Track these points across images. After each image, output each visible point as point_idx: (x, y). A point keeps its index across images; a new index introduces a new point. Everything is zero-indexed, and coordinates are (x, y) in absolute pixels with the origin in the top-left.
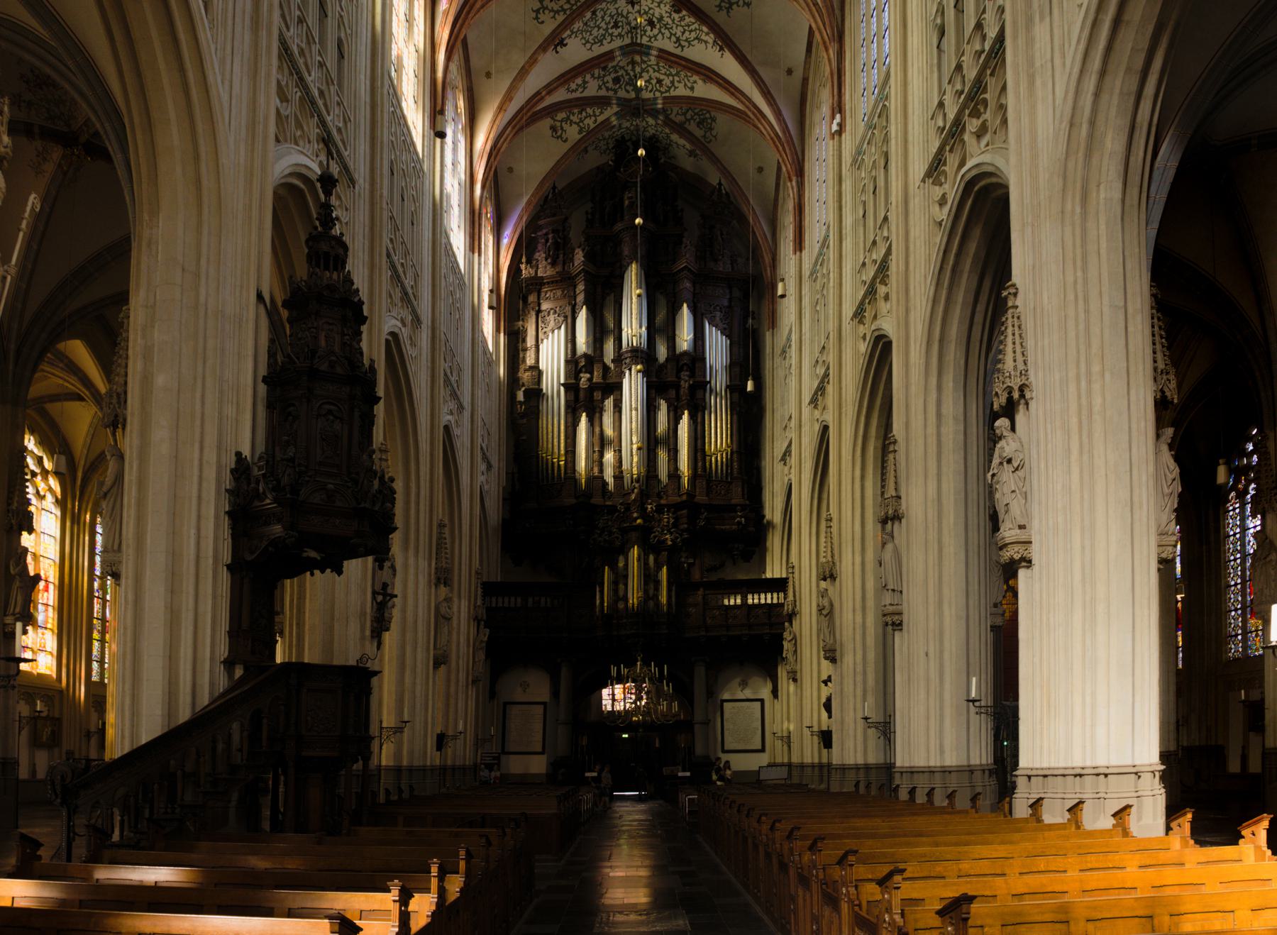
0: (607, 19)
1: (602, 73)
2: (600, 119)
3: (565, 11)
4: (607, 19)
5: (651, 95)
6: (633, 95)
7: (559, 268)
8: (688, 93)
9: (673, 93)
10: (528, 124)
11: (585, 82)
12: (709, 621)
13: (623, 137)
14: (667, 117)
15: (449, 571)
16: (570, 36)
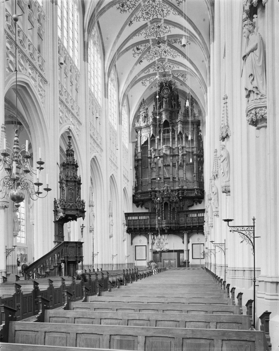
0: (153, 52)
1: (154, 66)
2: (155, 79)
3: (141, 53)
4: (153, 52)
5: (168, 70)
6: (163, 71)
7: (146, 123)
8: (178, 69)
9: (174, 69)
10: (132, 86)
11: (149, 70)
12: (187, 221)
13: (162, 82)
14: (173, 76)
15: (112, 213)
16: (143, 59)
